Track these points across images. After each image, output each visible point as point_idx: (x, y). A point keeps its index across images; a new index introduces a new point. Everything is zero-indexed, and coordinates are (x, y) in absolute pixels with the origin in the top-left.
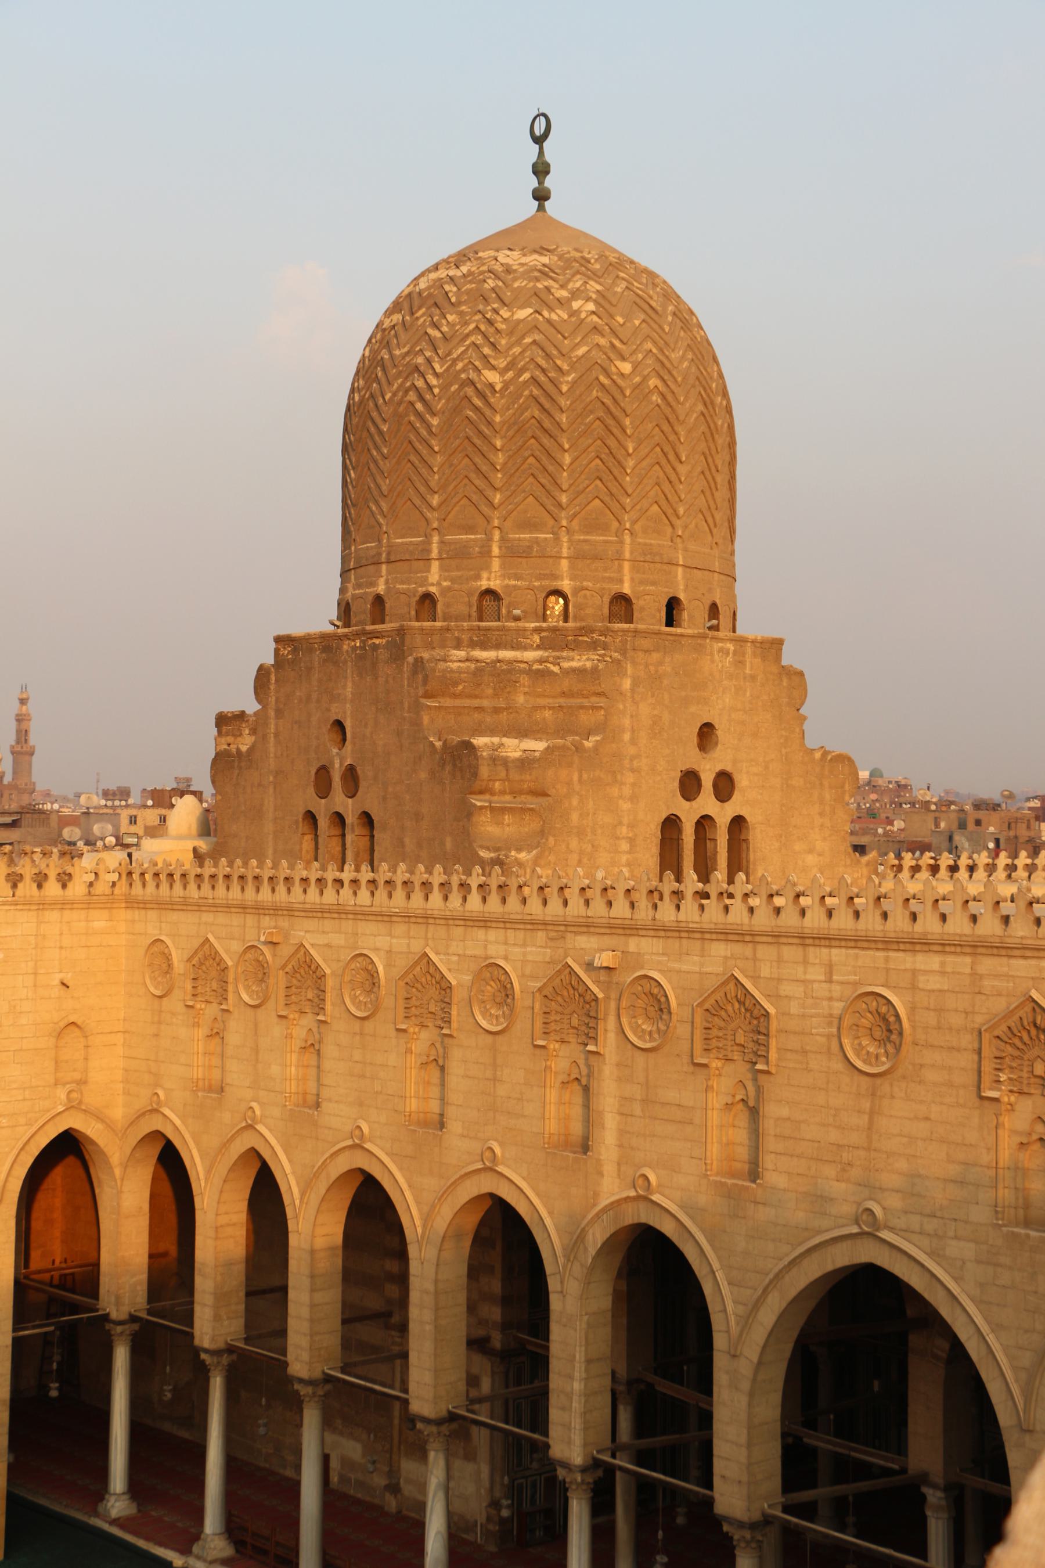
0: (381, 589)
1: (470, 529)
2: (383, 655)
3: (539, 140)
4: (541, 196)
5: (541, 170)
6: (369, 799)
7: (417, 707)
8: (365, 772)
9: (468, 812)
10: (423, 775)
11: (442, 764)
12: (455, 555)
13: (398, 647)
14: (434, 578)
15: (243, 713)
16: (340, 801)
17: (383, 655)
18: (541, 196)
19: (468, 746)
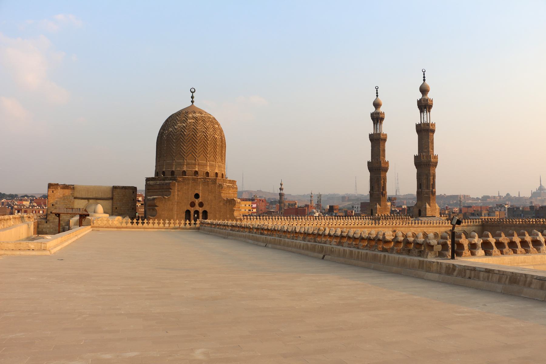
0: (197, 170)
1: (213, 162)
2: (210, 182)
3: (192, 92)
4: (192, 102)
5: (192, 97)
6: (206, 208)
7: (220, 193)
8: (205, 203)
9: (234, 211)
10: (221, 204)
11: (227, 203)
12: (211, 166)
13: (214, 181)
14: (208, 169)
15: (136, 188)
16: (197, 208)
17: (210, 182)
18: (192, 102)
19: (233, 200)
